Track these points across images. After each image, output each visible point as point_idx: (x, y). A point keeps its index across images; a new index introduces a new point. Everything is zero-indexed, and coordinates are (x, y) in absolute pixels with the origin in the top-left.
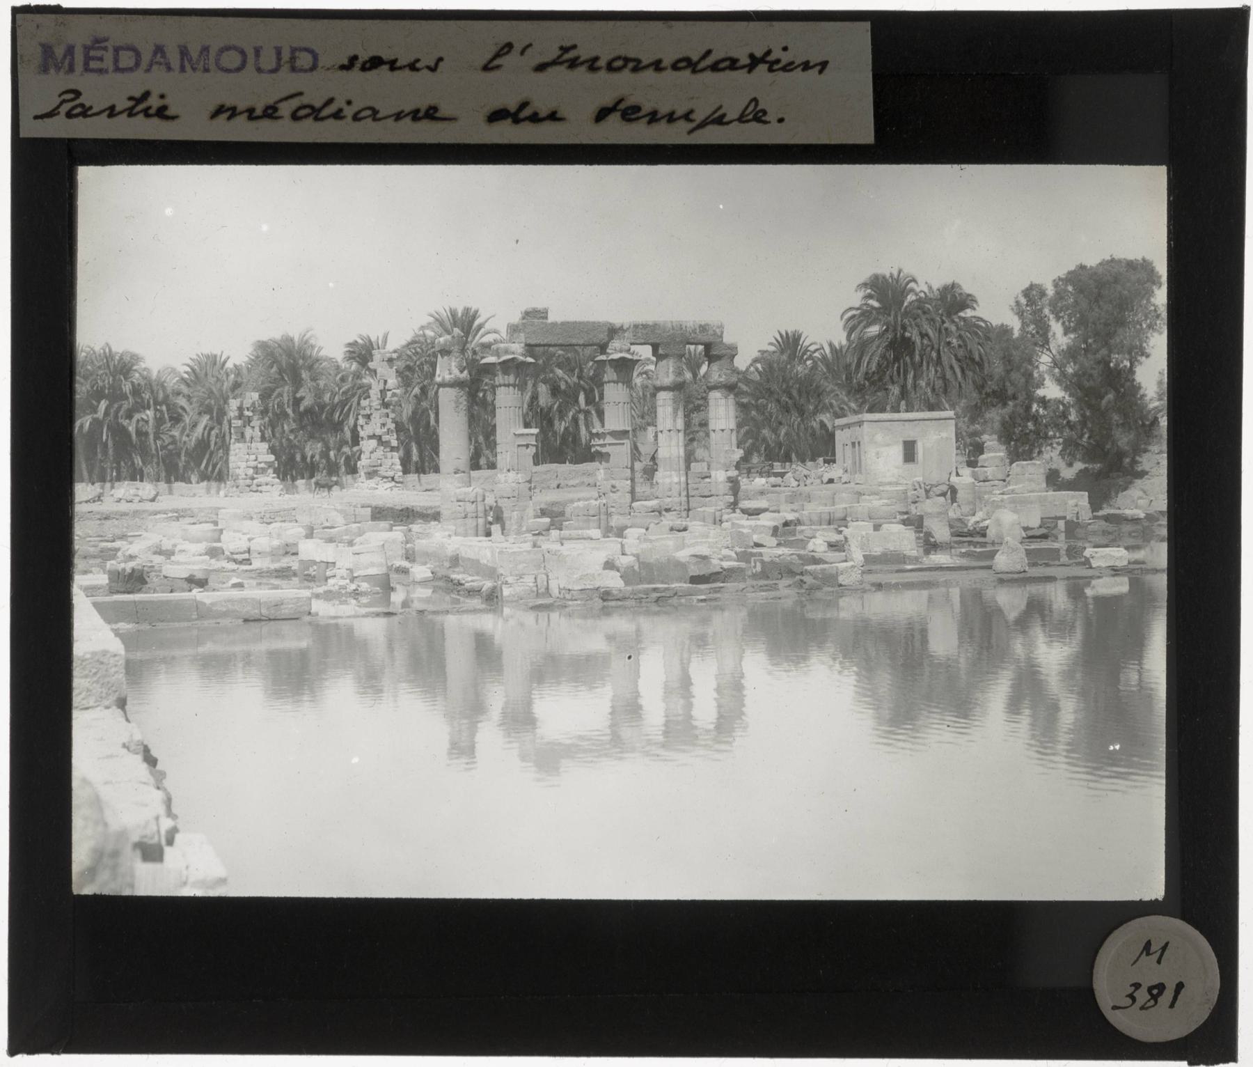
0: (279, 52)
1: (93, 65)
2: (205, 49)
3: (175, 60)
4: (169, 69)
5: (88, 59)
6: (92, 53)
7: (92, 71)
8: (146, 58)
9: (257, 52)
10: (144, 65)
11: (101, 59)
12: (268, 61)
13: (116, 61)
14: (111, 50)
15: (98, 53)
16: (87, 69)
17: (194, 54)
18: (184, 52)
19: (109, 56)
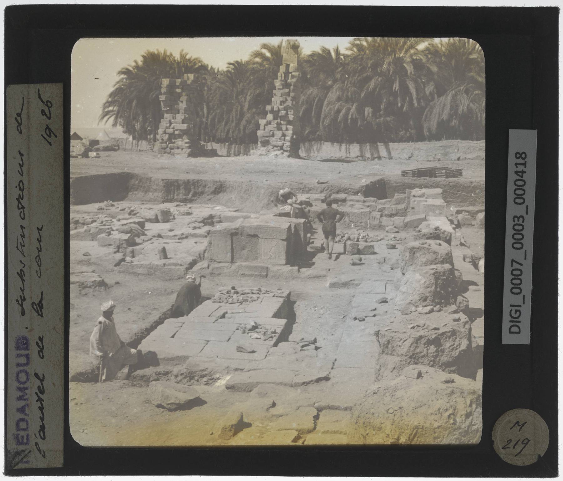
0: (19, 356)
1: (25, 440)
2: (19, 389)
3: (22, 403)
4: (27, 405)
5: (22, 443)
6: (20, 440)
7: (28, 439)
8: (22, 416)
9: (18, 365)
10: (26, 417)
11: (23, 437)
12: (23, 360)
13: (25, 430)
14: (18, 432)
15: (20, 440)
16: (27, 443)
17: (21, 394)
18: (20, 398)
19: (22, 433)
